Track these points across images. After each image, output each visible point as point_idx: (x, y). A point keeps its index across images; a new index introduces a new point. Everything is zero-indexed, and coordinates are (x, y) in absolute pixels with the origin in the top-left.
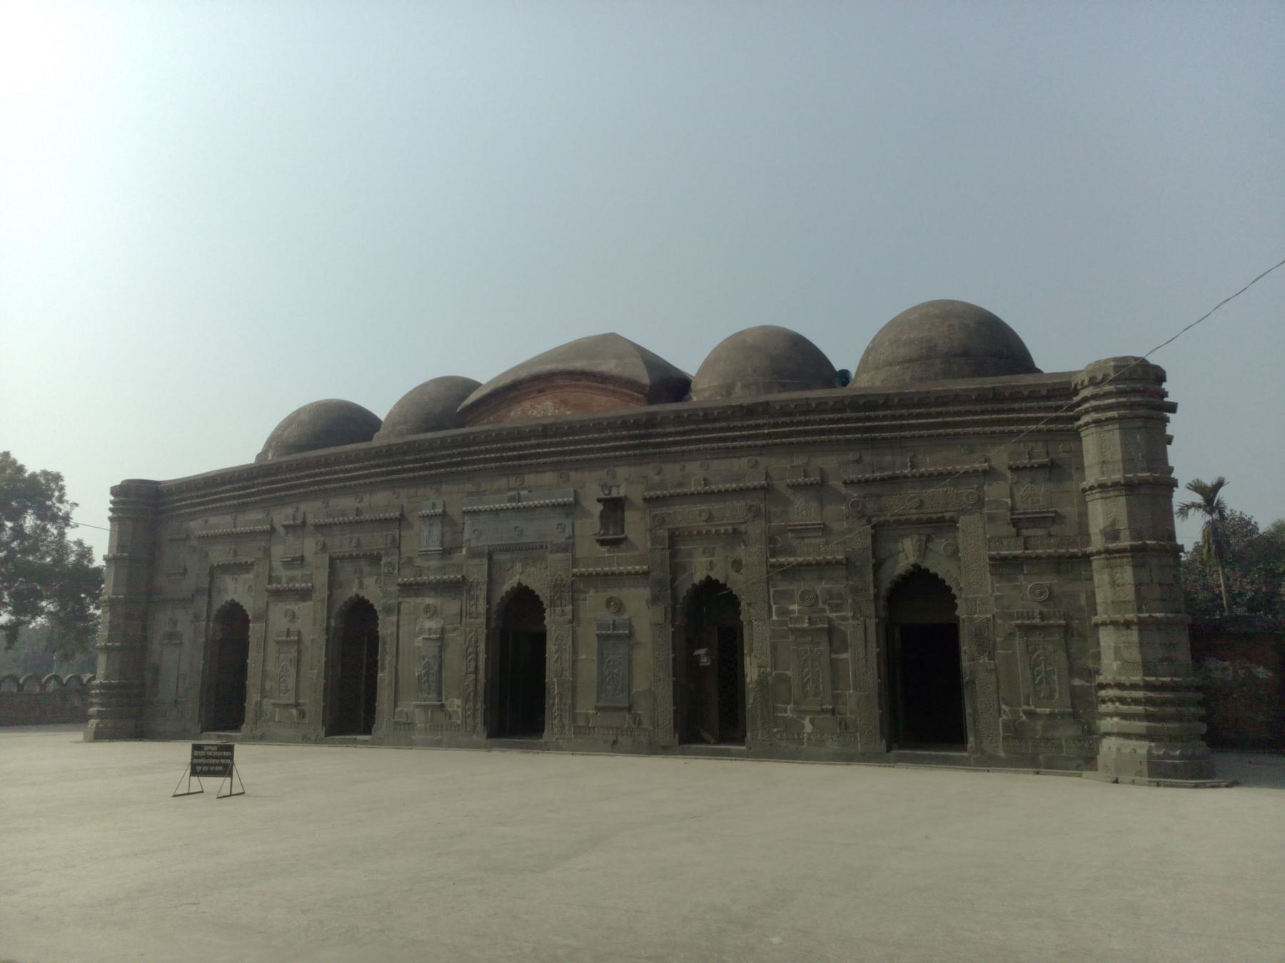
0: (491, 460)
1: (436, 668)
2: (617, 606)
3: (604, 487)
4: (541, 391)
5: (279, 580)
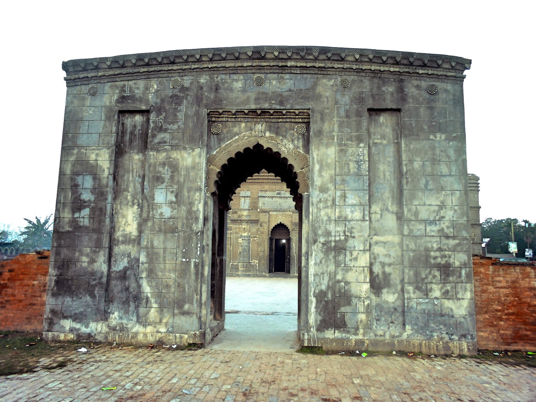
1: (247, 250)
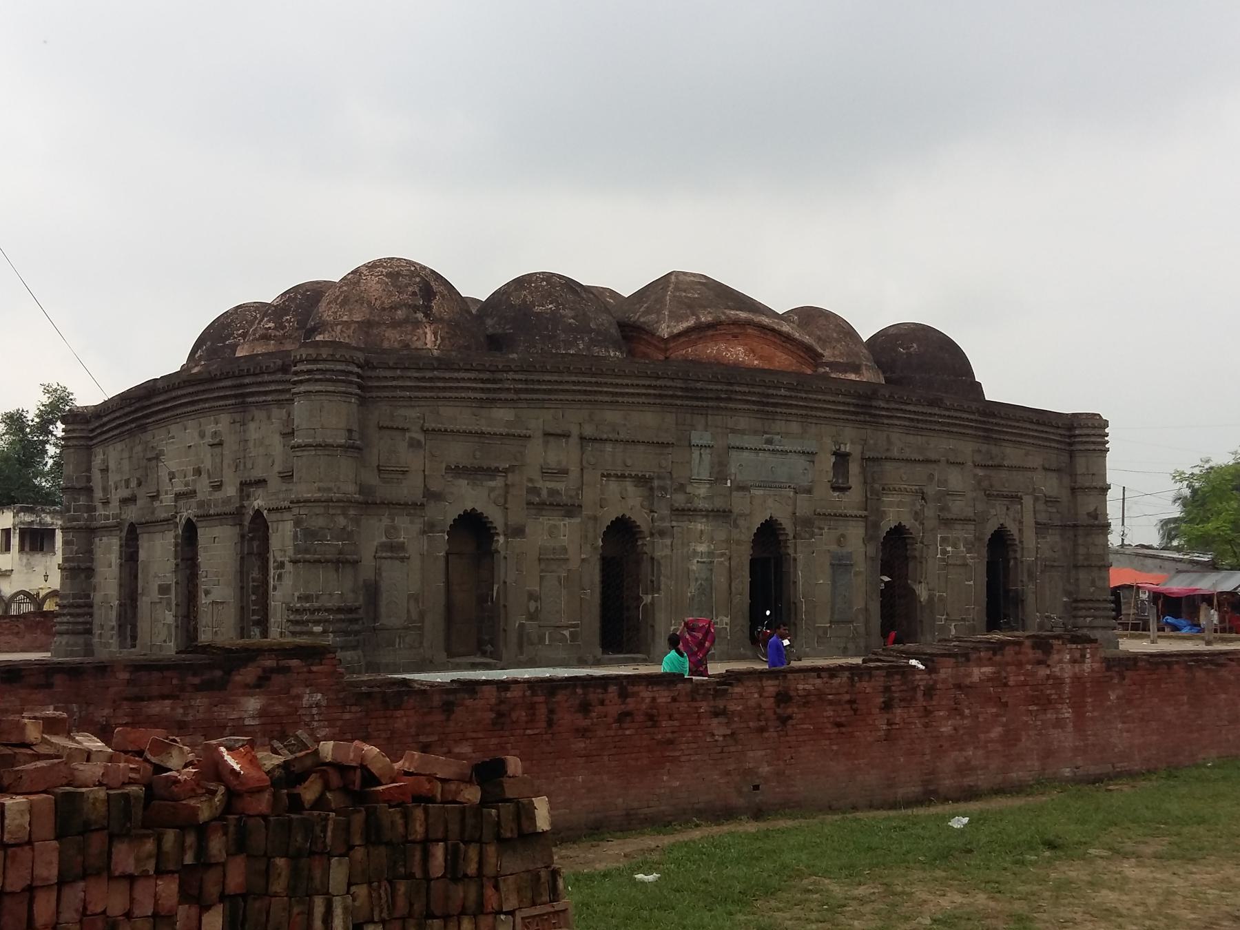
0: (754, 403)
2: (841, 540)
3: (836, 443)
4: (735, 336)
5: (535, 491)
